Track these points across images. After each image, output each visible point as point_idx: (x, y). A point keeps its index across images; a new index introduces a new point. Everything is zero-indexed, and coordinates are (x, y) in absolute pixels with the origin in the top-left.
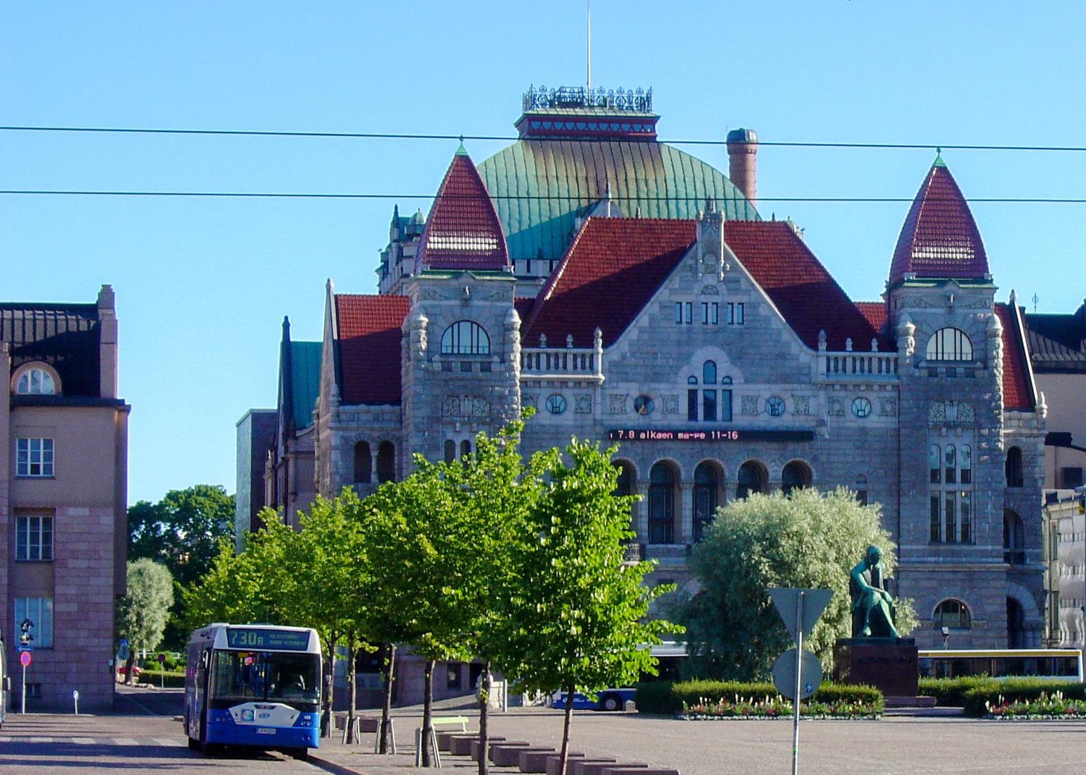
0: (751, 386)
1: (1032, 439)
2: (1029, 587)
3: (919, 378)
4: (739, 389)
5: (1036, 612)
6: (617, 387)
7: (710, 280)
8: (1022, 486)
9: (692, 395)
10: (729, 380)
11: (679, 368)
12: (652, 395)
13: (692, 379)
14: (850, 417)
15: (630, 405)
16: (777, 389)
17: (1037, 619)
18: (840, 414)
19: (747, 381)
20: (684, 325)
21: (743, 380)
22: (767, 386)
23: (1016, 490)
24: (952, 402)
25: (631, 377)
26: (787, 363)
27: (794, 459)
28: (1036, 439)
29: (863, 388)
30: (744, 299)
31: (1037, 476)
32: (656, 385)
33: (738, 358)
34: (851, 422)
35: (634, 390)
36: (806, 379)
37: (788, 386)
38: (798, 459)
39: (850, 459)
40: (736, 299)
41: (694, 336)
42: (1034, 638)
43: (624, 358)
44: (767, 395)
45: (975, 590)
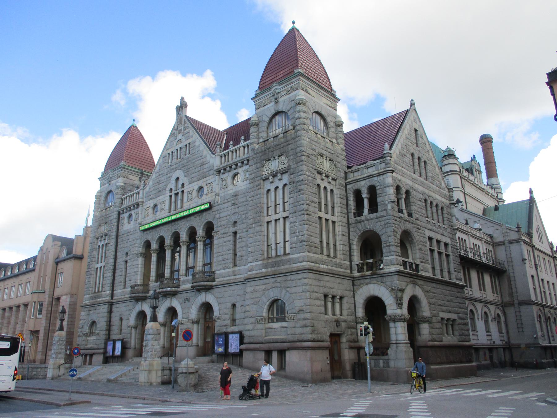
0: (191, 185)
1: (381, 177)
2: (387, 287)
3: (258, 149)
4: (186, 189)
5: (395, 306)
6: (147, 204)
7: (180, 137)
8: (376, 211)
9: (171, 196)
10: (183, 185)
11: (167, 185)
12: (158, 203)
13: (171, 190)
14: (230, 186)
15: (150, 210)
16: (200, 183)
17: (395, 311)
18: (226, 187)
19: (189, 184)
20: (170, 164)
21: (188, 183)
22: (197, 183)
23: (373, 215)
24: (274, 158)
25: (151, 197)
26: (205, 166)
27: (206, 221)
28: (384, 176)
29: (234, 167)
30: (190, 141)
31: (387, 202)
32: (158, 198)
33: (187, 173)
34: (231, 190)
35: (151, 204)
36: (212, 172)
37: (205, 179)
38: (208, 220)
39: (229, 213)
40: (187, 143)
41: (172, 167)
42: (395, 327)
43: (150, 188)
44: (196, 187)
45: (288, 289)
